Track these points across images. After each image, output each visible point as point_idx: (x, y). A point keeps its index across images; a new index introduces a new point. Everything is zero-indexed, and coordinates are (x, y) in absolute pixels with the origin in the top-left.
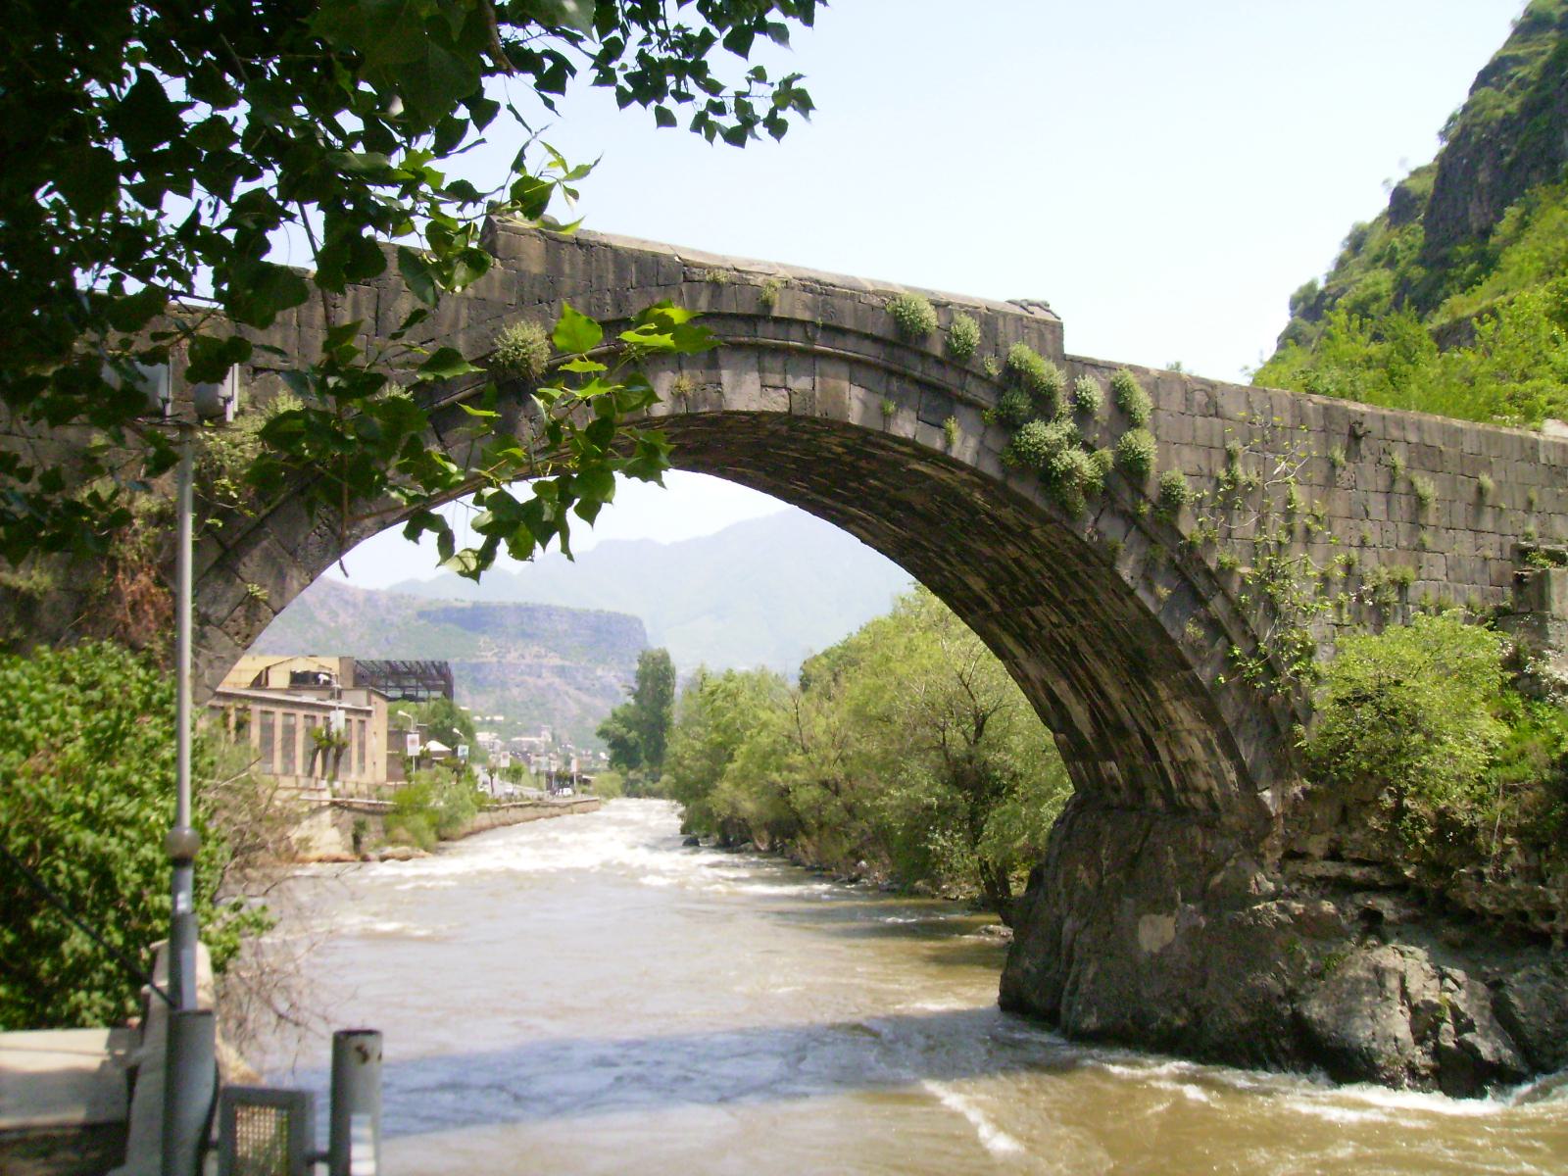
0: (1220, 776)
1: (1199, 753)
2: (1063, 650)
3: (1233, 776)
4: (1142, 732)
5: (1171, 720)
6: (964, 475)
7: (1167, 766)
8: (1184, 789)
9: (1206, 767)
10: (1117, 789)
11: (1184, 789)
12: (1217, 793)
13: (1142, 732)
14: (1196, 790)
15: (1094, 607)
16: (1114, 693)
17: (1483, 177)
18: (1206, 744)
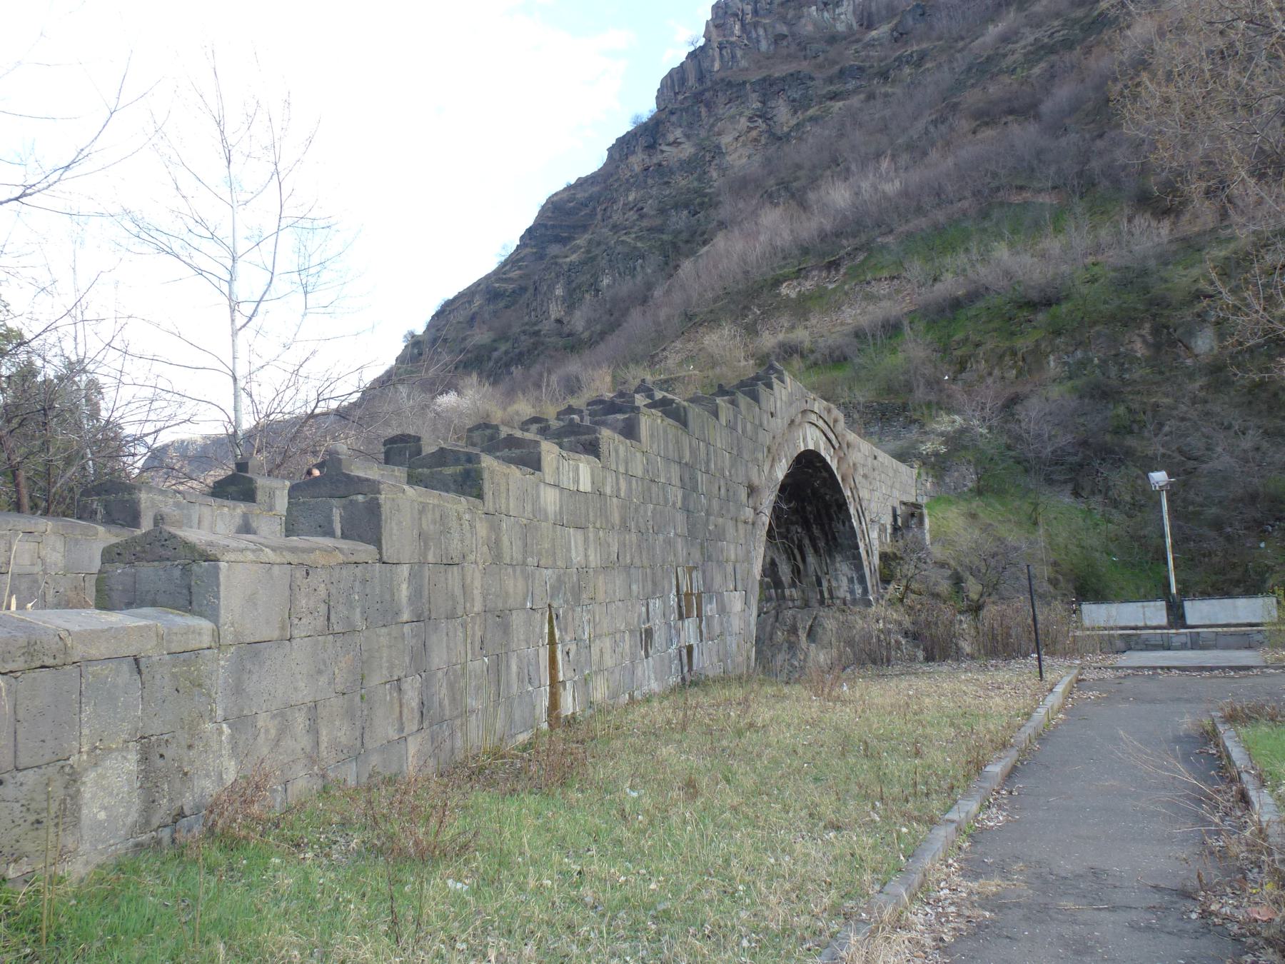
0: (852, 592)
1: (845, 582)
2: (793, 542)
3: (860, 591)
4: (817, 576)
5: (836, 570)
6: (825, 474)
7: (825, 590)
8: (832, 597)
9: (846, 588)
10: (793, 600)
11: (832, 597)
12: (848, 597)
13: (817, 576)
14: (838, 598)
15: (827, 527)
16: (811, 559)
17: (559, 291)
18: (851, 580)
